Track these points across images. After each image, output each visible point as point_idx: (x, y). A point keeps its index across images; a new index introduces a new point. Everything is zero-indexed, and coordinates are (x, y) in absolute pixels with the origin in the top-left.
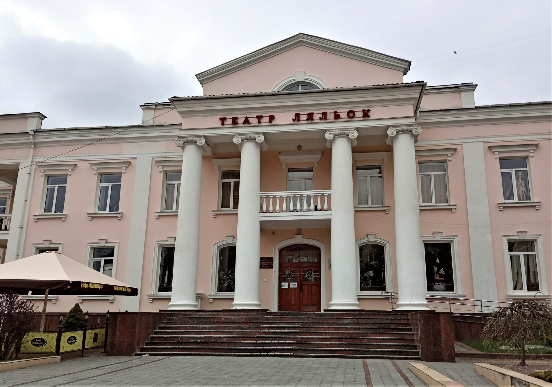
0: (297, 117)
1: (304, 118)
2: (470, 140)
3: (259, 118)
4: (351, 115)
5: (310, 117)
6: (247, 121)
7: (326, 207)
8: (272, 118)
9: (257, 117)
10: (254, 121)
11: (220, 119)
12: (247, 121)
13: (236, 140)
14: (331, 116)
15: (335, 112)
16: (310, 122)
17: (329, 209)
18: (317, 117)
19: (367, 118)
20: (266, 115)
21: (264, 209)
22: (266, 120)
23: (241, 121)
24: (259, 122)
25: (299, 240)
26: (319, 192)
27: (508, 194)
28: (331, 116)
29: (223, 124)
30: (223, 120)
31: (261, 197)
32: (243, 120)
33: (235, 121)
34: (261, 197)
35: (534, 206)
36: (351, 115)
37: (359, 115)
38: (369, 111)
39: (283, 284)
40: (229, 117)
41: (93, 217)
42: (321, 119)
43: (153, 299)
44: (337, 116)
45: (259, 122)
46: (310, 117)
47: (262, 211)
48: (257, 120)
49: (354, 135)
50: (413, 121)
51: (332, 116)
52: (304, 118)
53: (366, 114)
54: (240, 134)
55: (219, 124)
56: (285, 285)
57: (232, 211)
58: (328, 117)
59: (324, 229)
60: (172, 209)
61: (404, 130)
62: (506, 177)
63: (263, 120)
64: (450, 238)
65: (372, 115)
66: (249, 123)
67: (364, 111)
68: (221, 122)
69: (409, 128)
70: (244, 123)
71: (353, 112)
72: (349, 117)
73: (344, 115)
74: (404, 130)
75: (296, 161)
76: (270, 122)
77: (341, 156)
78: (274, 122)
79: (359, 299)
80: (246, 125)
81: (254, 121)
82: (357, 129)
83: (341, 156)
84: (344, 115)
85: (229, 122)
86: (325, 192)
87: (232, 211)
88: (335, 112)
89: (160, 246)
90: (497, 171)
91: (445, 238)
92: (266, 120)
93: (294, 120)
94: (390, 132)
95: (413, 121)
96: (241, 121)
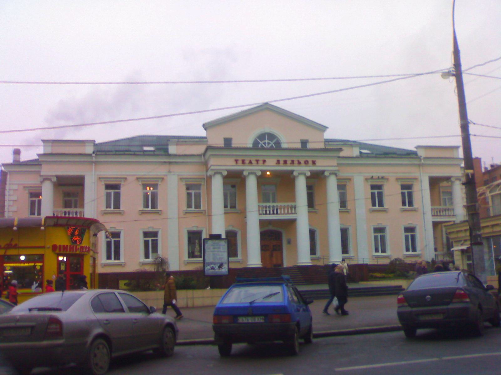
0: (278, 162)
1: (282, 162)
4: (306, 163)
5: (285, 162)
6: (250, 162)
8: (264, 161)
10: (254, 162)
12: (250, 162)
13: (245, 173)
14: (296, 162)
16: (285, 165)
17: (295, 213)
20: (261, 159)
22: (261, 162)
23: (247, 162)
24: (257, 163)
25: (271, 228)
26: (290, 204)
27: (374, 204)
28: (296, 162)
29: (237, 163)
30: (236, 161)
33: (243, 162)
34: (259, 206)
35: (385, 211)
36: (306, 162)
37: (310, 163)
40: (240, 159)
41: (143, 213)
42: (291, 164)
43: (187, 263)
44: (299, 163)
45: (257, 163)
46: (285, 162)
47: (260, 214)
49: (309, 174)
50: (336, 168)
52: (282, 162)
53: (314, 163)
54: (247, 170)
55: (234, 163)
58: (295, 163)
59: (292, 223)
60: (192, 208)
62: (373, 195)
63: (259, 162)
65: (317, 164)
73: (302, 162)
74: (334, 173)
77: (301, 185)
78: (266, 164)
79: (311, 260)
80: (250, 164)
81: (254, 162)
82: (310, 171)
83: (301, 185)
84: (302, 162)
85: (240, 162)
86: (293, 204)
87: (229, 210)
89: (187, 231)
90: (370, 191)
92: (261, 162)
93: (276, 163)
94: (326, 174)
95: (336, 168)
96: (247, 162)
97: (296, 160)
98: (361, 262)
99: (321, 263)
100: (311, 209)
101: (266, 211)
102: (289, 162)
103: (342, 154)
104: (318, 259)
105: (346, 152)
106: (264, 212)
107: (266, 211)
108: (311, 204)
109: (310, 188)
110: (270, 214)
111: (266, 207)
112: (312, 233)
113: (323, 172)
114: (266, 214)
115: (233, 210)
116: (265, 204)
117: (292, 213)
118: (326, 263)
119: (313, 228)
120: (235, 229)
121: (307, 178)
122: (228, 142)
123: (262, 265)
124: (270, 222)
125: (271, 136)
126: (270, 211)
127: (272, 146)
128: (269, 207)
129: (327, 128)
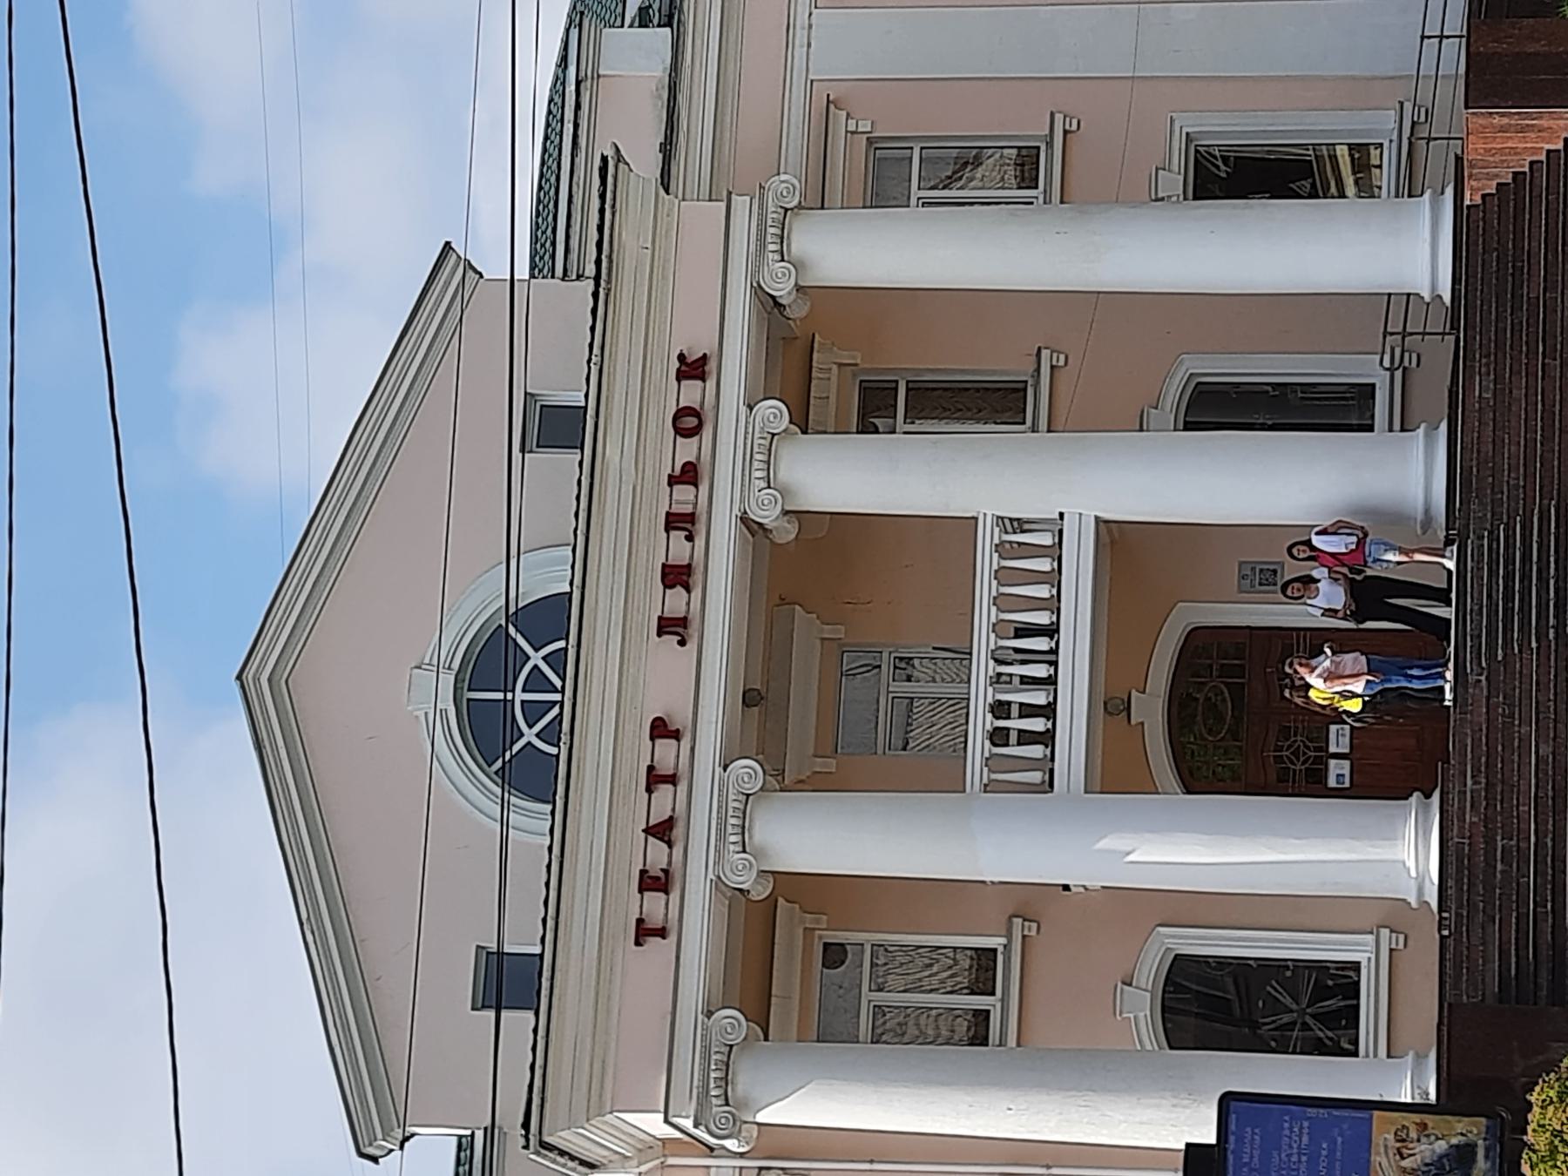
0: (673, 626)
1: (676, 603)
2: (800, 52)
3: (655, 779)
4: (691, 422)
6: (662, 831)
7: (1046, 539)
8: (660, 729)
9: (649, 790)
11: (638, 943)
12: (662, 831)
15: (673, 481)
16: (697, 578)
18: (680, 549)
19: (712, 366)
21: (1036, 777)
23: (658, 853)
24: (672, 780)
25: (1151, 710)
26: (987, 561)
29: (662, 933)
30: (644, 932)
31: (986, 789)
32: (657, 848)
33: (654, 882)
34: (986, 789)
36: (688, 422)
37: (691, 393)
38: (681, 357)
39: (1332, 783)
42: (690, 538)
44: (688, 475)
45: (672, 780)
48: (665, 790)
49: (773, 412)
51: (684, 492)
52: (676, 603)
53: (693, 368)
56: (1338, 771)
57: (1004, 1000)
61: (775, 234)
63: (665, 767)
64: (1178, 144)
66: (669, 823)
67: (681, 376)
68: (654, 942)
69: (773, 215)
70: (670, 845)
71: (681, 413)
72: (695, 431)
73: (687, 450)
75: (844, 656)
76: (676, 735)
78: (681, 719)
80: (678, 832)
84: (687, 450)
86: (987, 538)
87: (1004, 1000)
88: (673, 481)
91: (1177, 161)
93: (682, 643)
95: (741, 203)
97: (662, 501)
98: (1454, 58)
99: (1439, 356)
100: (1039, 402)
101: (1026, 738)
102: (680, 549)
103: (644, 162)
104: (1403, 372)
105: (627, 125)
106: (1036, 751)
107: (1026, 738)
108: (995, 403)
109: (874, 408)
110: (1049, 711)
111: (998, 737)
112: (1218, 408)
113: (767, 305)
114: (1047, 738)
115: (1008, 974)
116: (978, 745)
117: (1055, 552)
118: (1438, 322)
119: (1173, 392)
120: (1150, 970)
121: (802, 422)
122: (508, 982)
123: (1428, 796)
124: (1112, 707)
125: (489, 661)
126: (1028, 711)
127: (557, 661)
128: (1000, 709)
129: (448, 244)
